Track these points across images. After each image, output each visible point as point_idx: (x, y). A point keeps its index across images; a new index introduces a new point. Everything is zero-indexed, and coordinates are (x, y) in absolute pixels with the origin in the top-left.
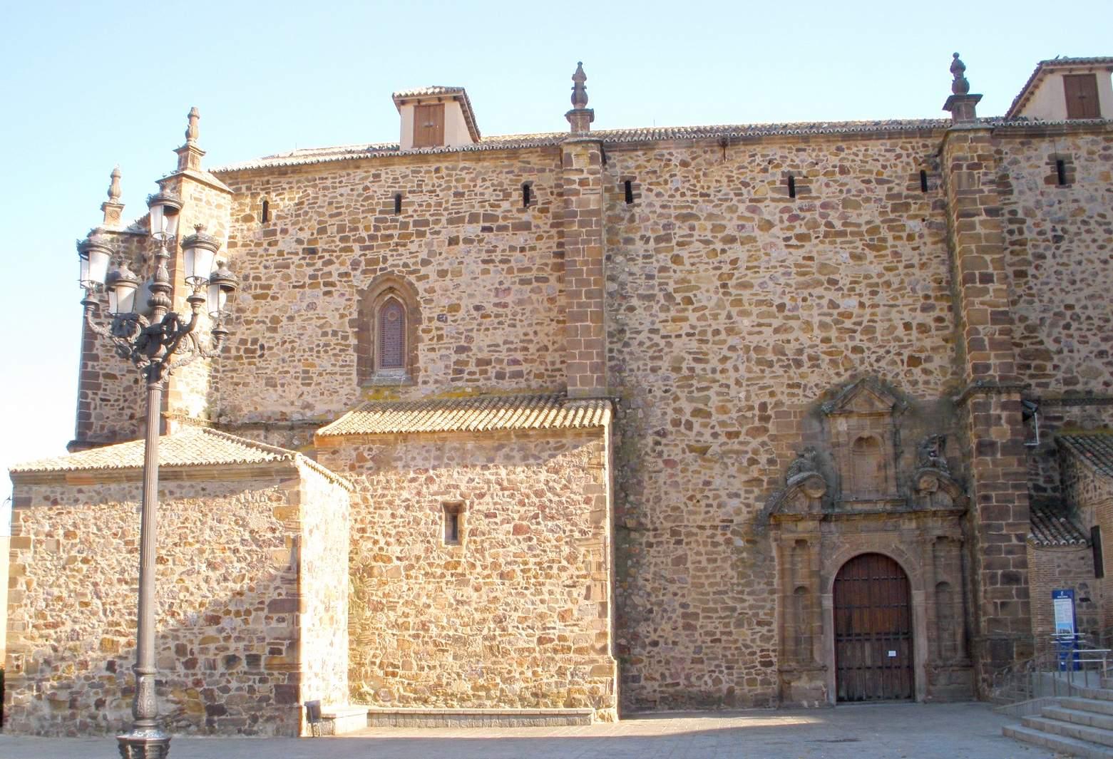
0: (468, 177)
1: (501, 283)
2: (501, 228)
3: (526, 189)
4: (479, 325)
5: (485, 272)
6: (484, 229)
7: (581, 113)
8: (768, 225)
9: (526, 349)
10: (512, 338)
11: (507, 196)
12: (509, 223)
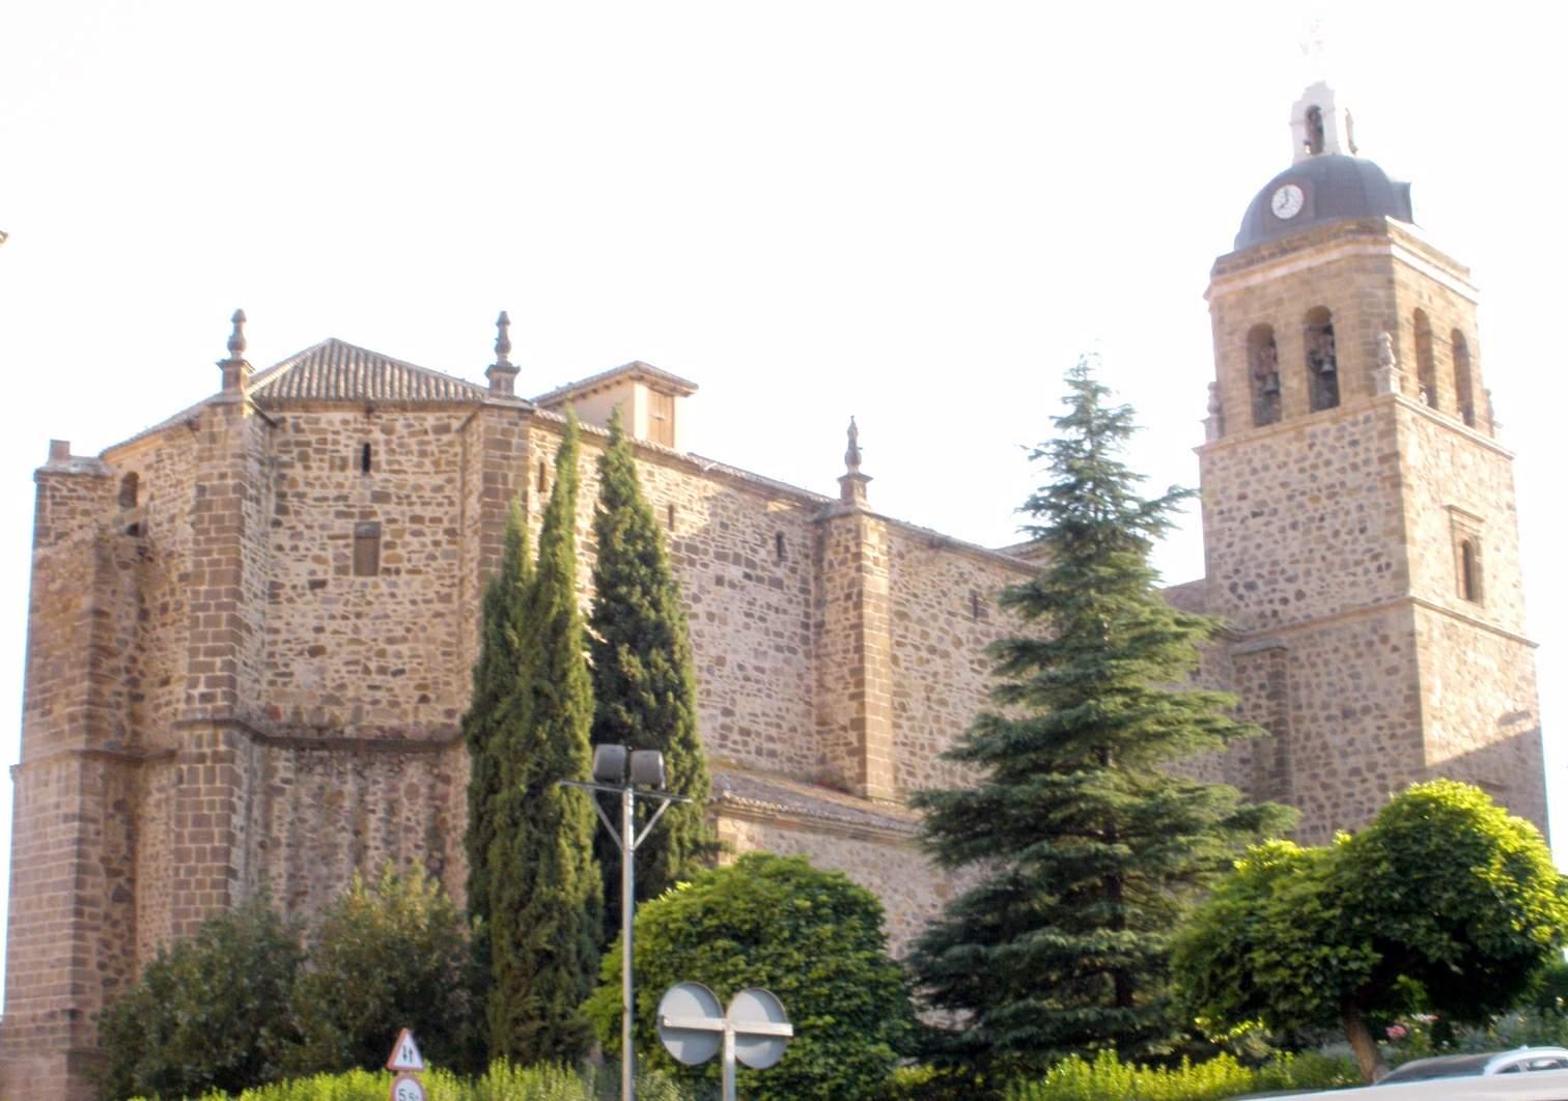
0: (732, 506)
1: (760, 644)
2: (760, 580)
3: (779, 538)
4: (742, 687)
5: (747, 627)
6: (747, 576)
7: (503, 373)
8: (958, 643)
9: (779, 726)
10: (768, 711)
11: (764, 542)
12: (765, 575)
